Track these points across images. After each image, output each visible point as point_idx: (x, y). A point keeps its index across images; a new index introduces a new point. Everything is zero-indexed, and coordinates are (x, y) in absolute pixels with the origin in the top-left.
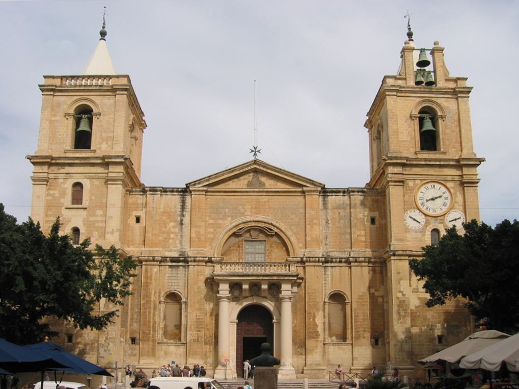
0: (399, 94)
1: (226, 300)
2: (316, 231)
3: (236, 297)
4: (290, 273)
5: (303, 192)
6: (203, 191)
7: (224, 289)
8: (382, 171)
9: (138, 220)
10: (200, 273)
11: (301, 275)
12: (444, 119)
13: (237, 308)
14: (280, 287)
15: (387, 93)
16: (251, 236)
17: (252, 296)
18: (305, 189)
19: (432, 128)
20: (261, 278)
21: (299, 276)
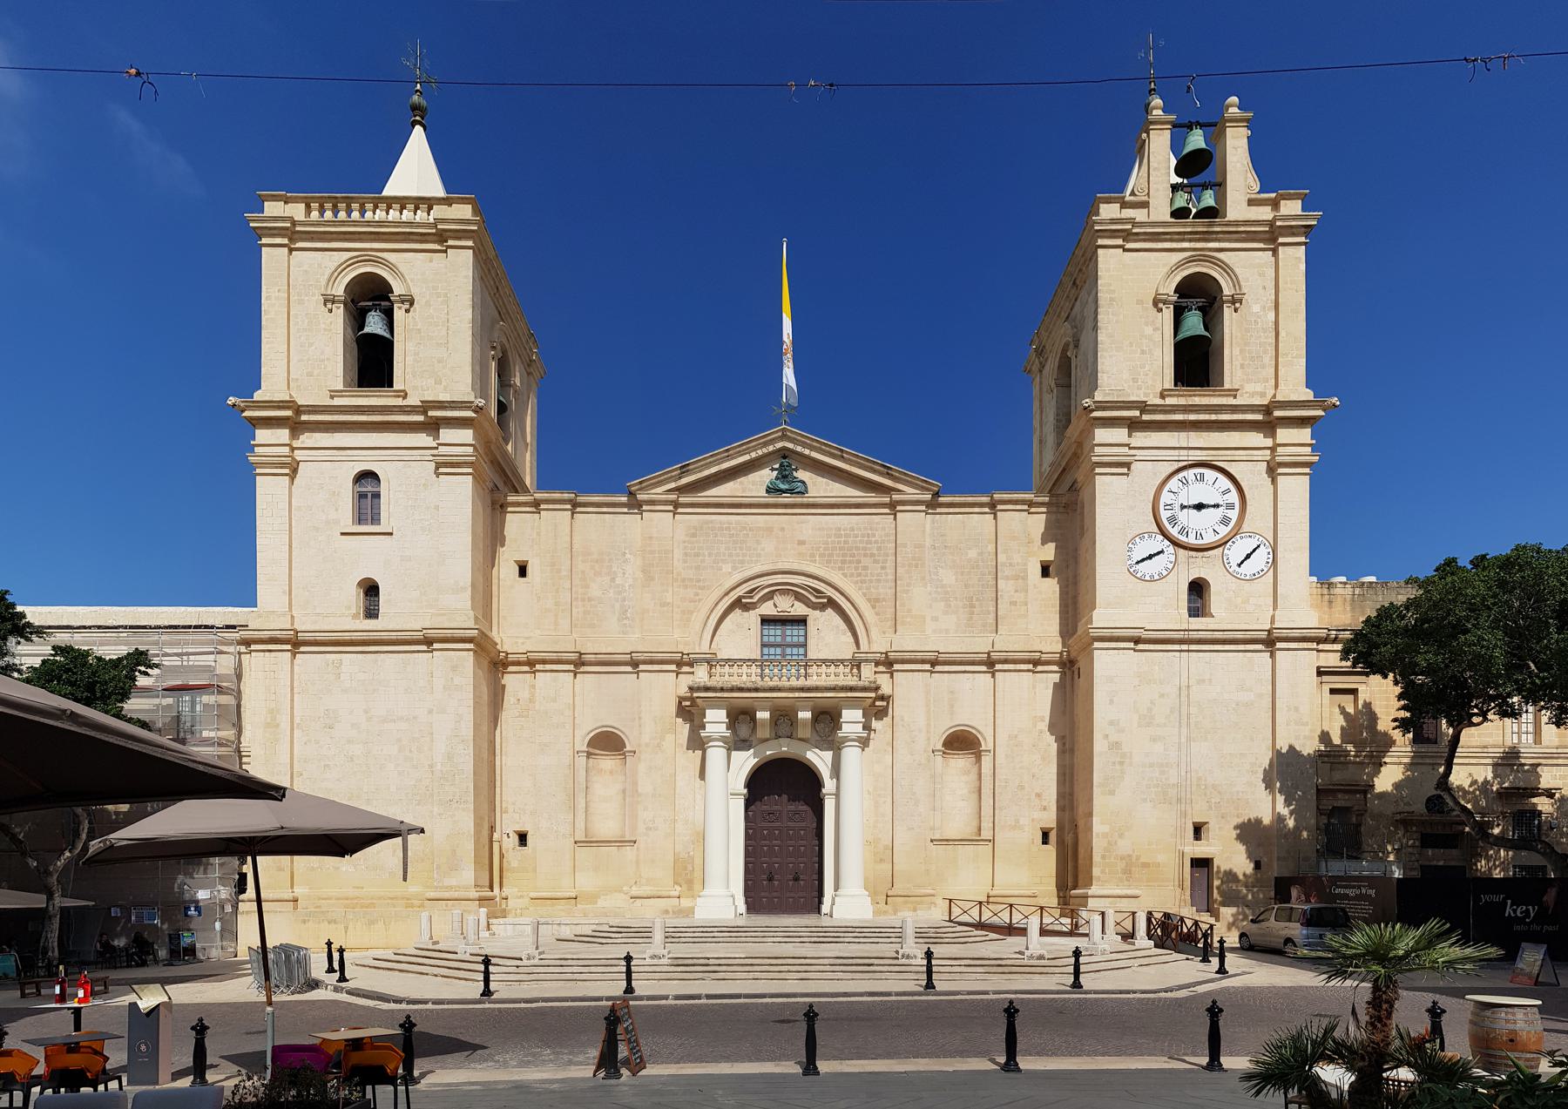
0: (1129, 246)
1: (721, 744)
2: (918, 597)
3: (744, 741)
4: (861, 684)
5: (892, 506)
6: (666, 503)
7: (716, 721)
8: (1074, 446)
9: (523, 571)
10: (666, 688)
11: (886, 690)
12: (1237, 305)
13: (746, 761)
14: (840, 716)
15: (1100, 242)
16: (776, 606)
17: (778, 737)
18: (896, 497)
19: (1201, 331)
20: (797, 695)
21: (880, 692)
